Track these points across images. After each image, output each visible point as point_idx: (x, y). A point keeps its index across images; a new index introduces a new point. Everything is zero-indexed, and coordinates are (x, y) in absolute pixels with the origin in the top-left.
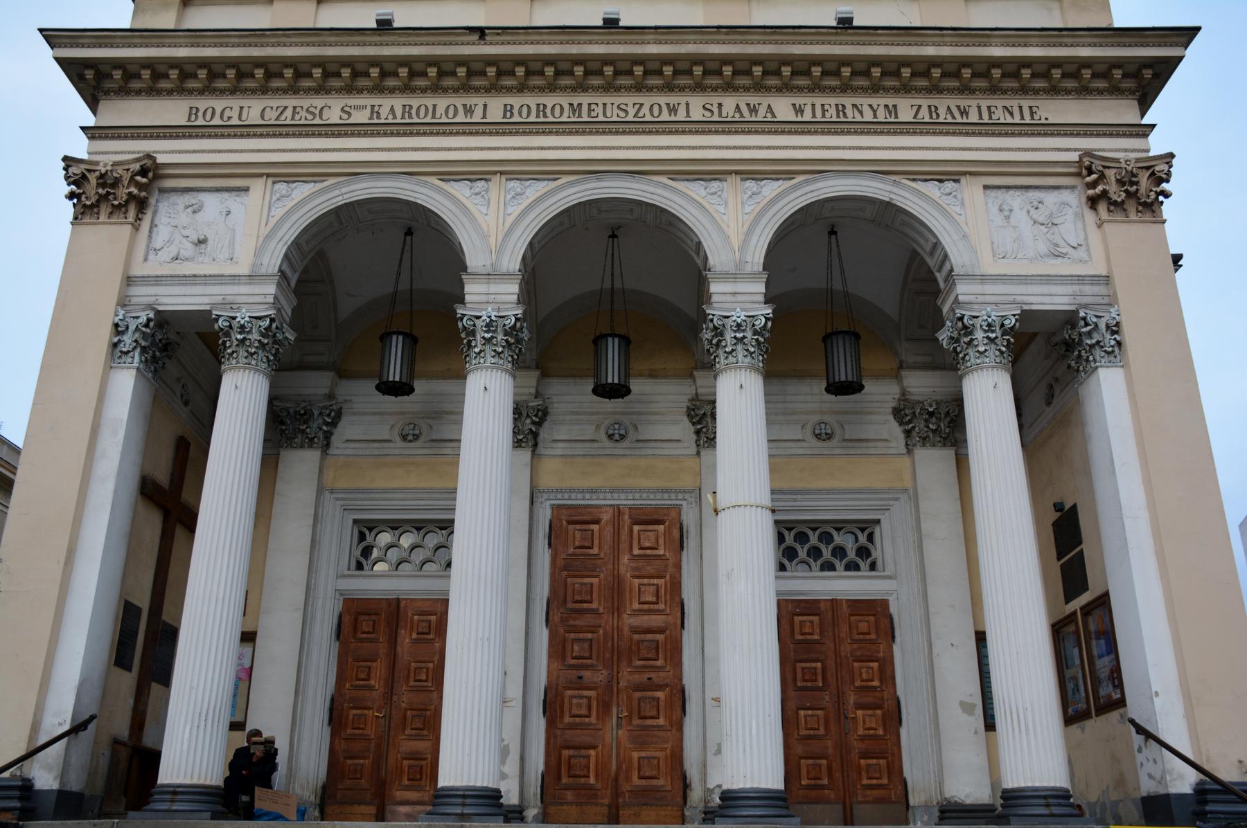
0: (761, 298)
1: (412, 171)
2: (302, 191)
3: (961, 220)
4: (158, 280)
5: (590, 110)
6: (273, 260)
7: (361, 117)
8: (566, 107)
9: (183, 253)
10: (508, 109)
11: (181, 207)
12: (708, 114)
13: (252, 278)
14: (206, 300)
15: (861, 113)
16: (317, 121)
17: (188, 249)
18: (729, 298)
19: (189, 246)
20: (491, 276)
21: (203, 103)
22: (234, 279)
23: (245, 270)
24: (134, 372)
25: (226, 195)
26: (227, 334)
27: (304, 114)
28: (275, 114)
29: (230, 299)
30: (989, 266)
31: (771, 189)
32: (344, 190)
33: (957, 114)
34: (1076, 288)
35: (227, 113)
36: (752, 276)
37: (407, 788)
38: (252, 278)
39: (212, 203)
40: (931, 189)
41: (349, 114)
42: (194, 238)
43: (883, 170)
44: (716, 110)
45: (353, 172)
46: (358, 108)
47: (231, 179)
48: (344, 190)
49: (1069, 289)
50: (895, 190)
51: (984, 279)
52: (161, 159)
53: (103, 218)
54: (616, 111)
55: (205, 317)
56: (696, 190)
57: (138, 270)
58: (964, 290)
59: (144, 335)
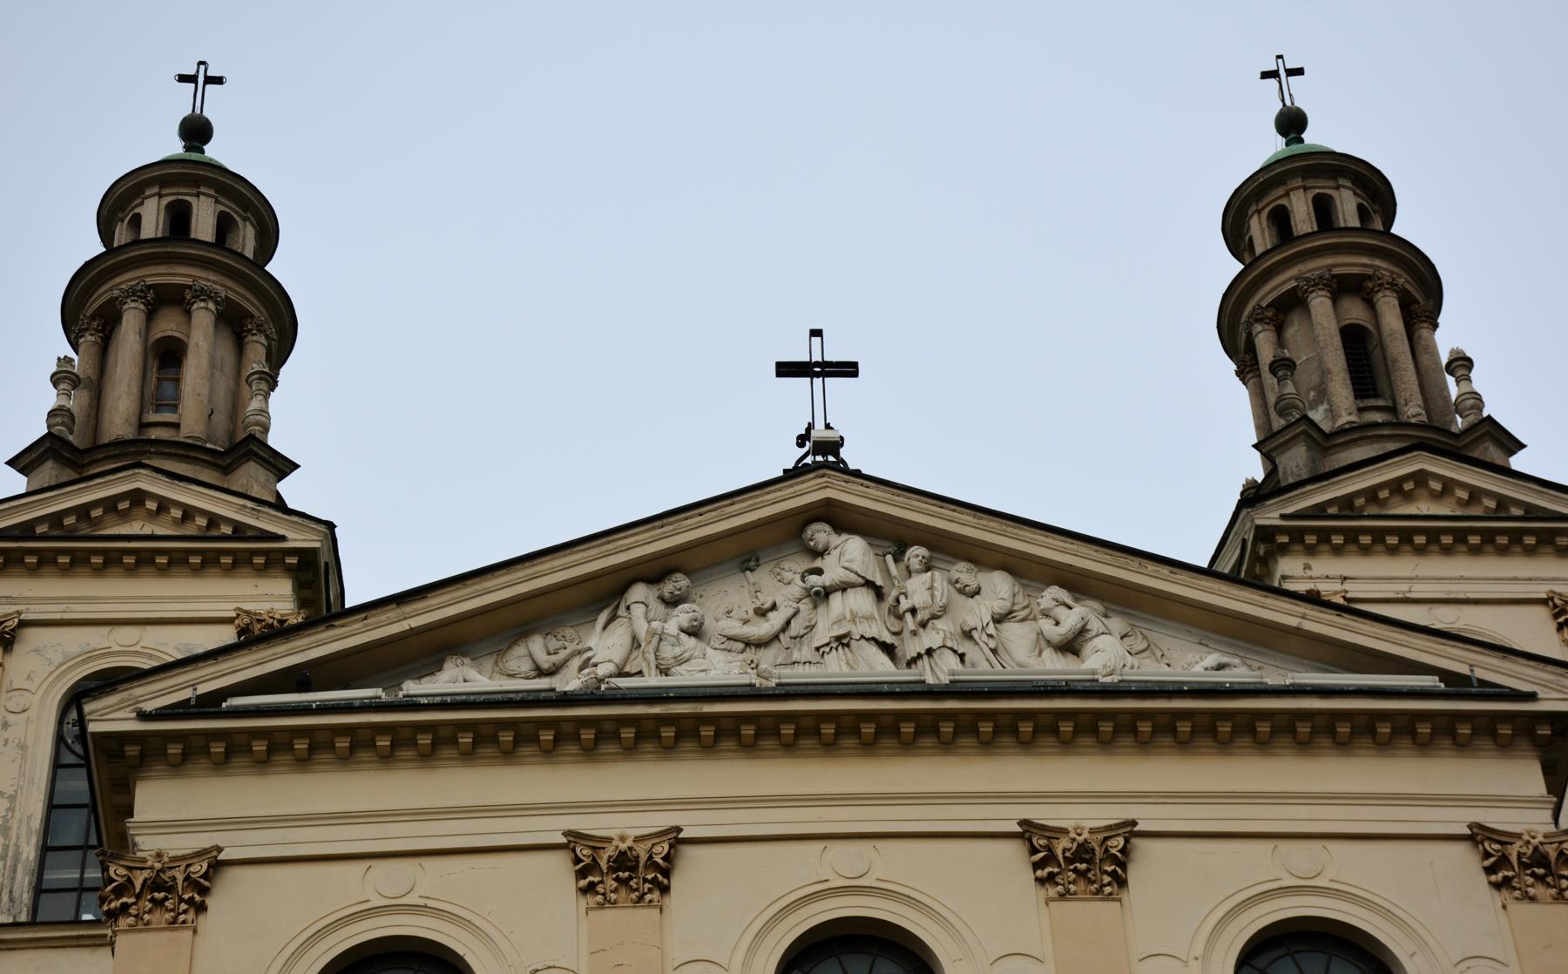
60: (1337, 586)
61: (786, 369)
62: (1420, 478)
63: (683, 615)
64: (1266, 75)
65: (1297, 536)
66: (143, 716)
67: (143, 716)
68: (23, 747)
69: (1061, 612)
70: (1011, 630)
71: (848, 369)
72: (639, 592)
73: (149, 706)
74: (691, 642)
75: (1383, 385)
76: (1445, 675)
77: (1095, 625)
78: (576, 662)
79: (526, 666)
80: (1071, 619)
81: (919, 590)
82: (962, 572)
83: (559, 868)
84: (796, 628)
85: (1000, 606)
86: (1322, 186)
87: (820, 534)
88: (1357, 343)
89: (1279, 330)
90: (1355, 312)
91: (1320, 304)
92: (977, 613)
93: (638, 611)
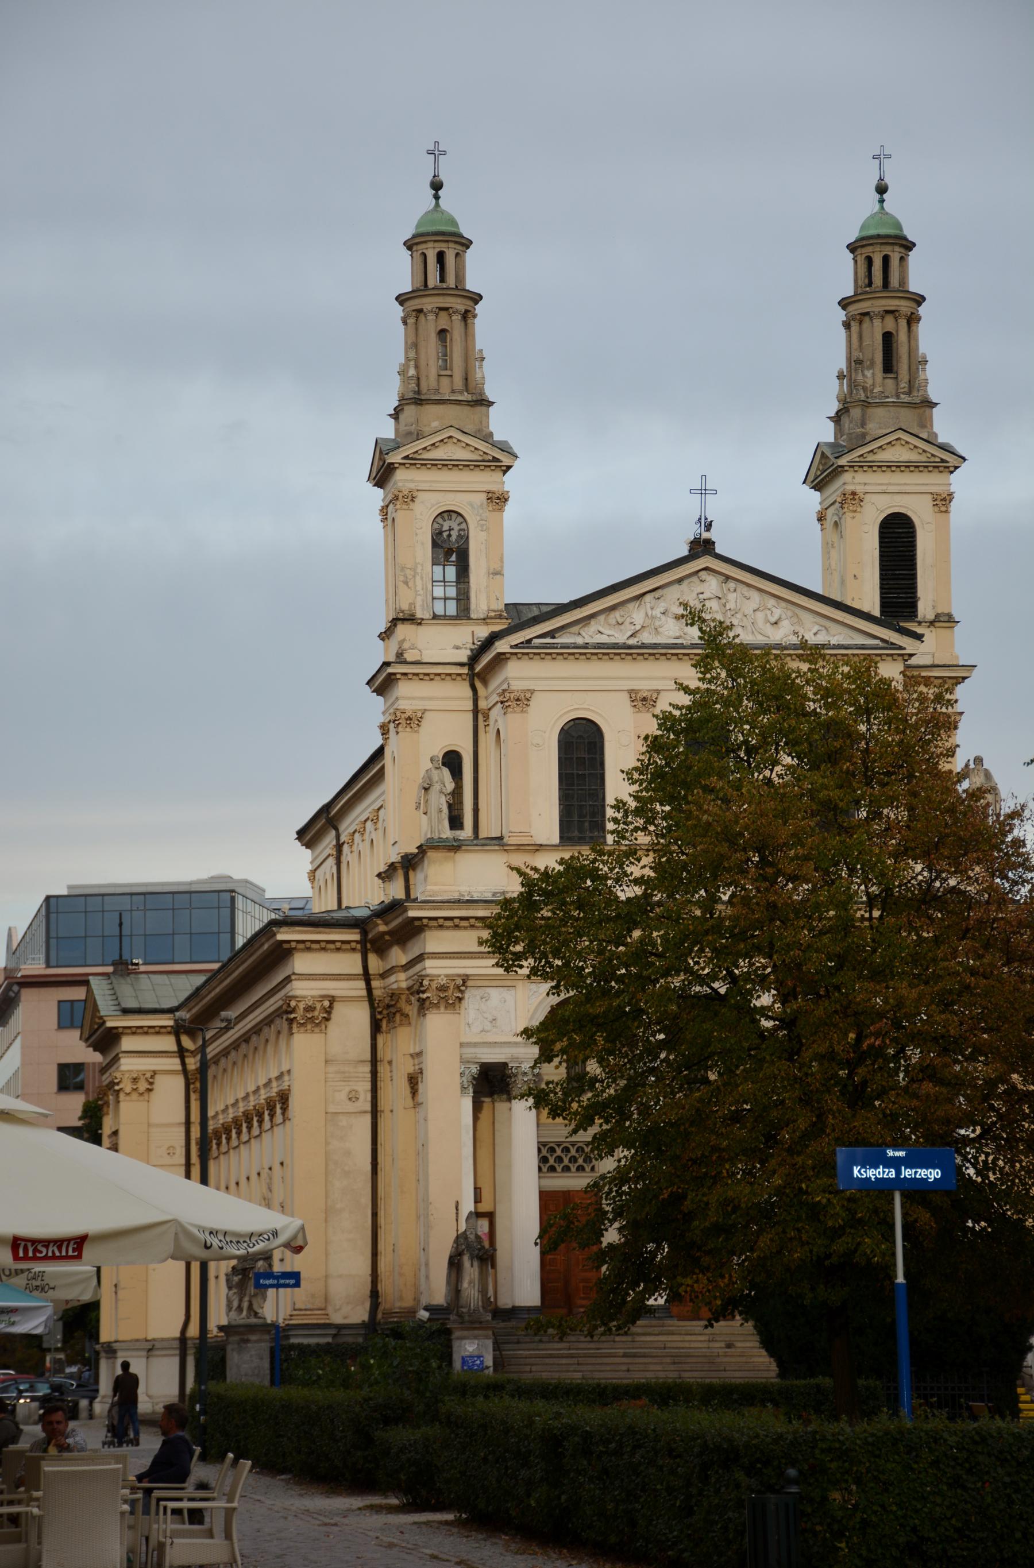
4: (475, 1045)
9: (486, 1028)
11: (478, 998)
14: (503, 1056)
17: (488, 1026)
19: (489, 1024)
24: (471, 1099)
25: (502, 989)
26: (516, 1075)
29: (516, 1055)
37: (584, 1299)
42: (490, 1018)
52: (469, 972)
53: (442, 1009)
57: (464, 1040)
59: (474, 1078)
60: (862, 487)
63: (662, 606)
66: (512, 647)
67: (512, 647)
68: (423, 544)
69: (774, 609)
70: (758, 613)
72: (648, 598)
73: (513, 643)
74: (663, 617)
75: (895, 369)
76: (883, 640)
77: (784, 616)
79: (614, 622)
80: (777, 613)
81: (732, 597)
82: (745, 590)
83: (626, 696)
85: (756, 606)
86: (887, 250)
87: (703, 575)
88: (888, 338)
89: (861, 322)
90: (890, 324)
91: (877, 322)
92: (749, 607)
93: (648, 605)
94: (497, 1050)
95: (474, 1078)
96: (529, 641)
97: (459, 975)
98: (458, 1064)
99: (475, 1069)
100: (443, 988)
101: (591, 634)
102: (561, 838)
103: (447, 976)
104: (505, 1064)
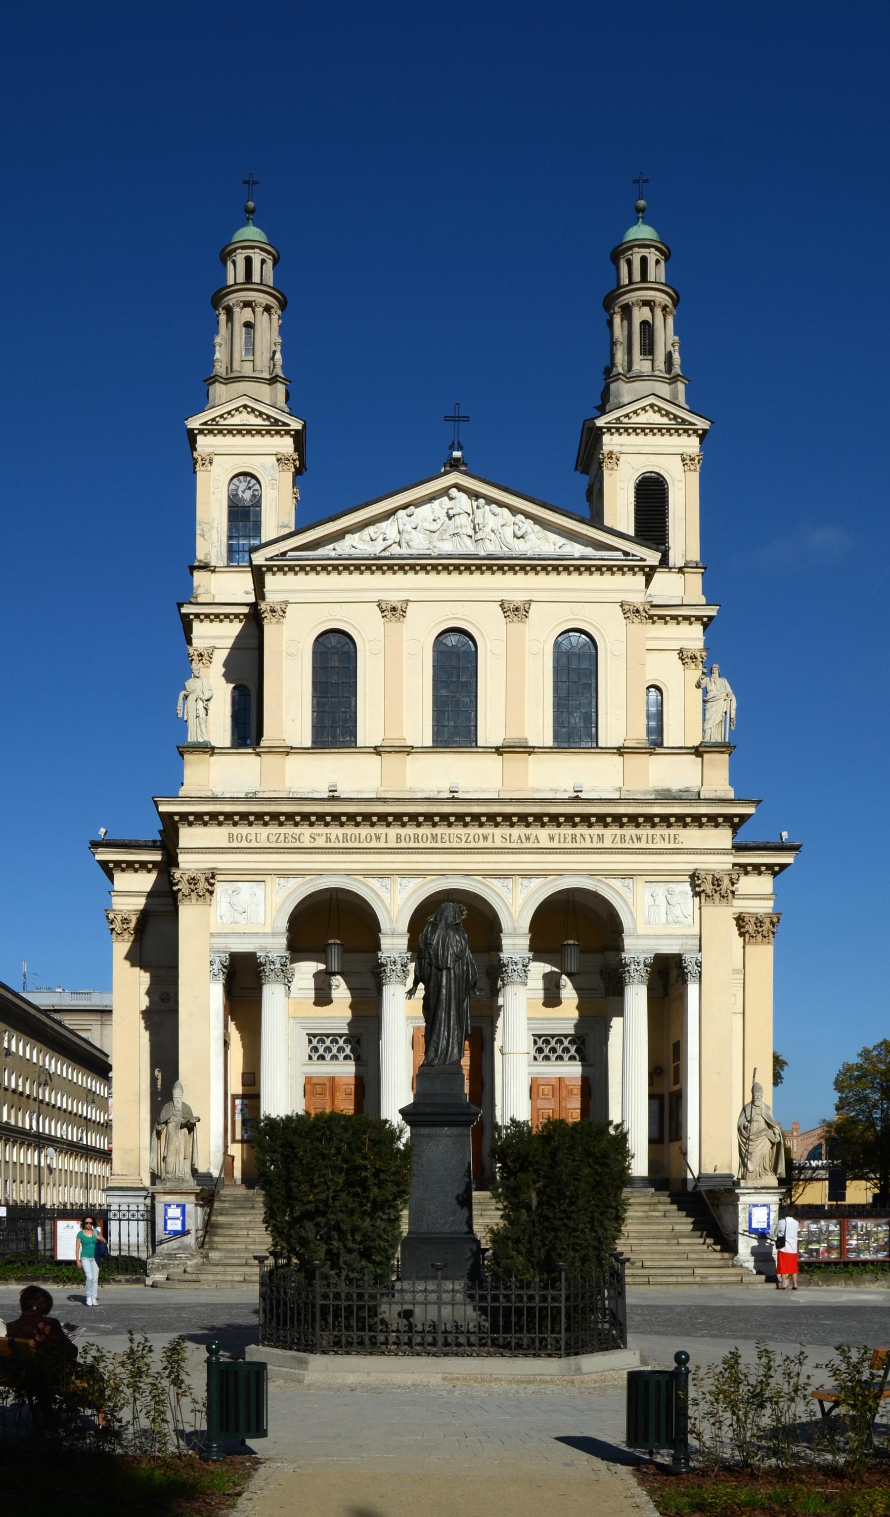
0: (527, 947)
1: (349, 874)
2: (293, 883)
3: (630, 901)
4: (226, 935)
5: (442, 838)
6: (283, 924)
7: (321, 842)
8: (429, 836)
10: (398, 838)
12: (504, 840)
13: (274, 935)
14: (252, 946)
15: (584, 839)
16: (298, 845)
18: (511, 947)
20: (393, 934)
21: (236, 830)
22: (265, 935)
23: (268, 930)
26: (265, 965)
27: (290, 838)
28: (275, 839)
30: (640, 931)
31: (535, 882)
32: (315, 883)
33: (635, 840)
34: (684, 941)
35: (249, 838)
36: (524, 935)
38: (274, 935)
39: (245, 888)
40: (616, 883)
41: (315, 839)
42: (241, 911)
43: (592, 874)
44: (508, 838)
45: (319, 873)
46: (319, 835)
47: (256, 876)
48: (315, 883)
49: (680, 942)
50: (599, 884)
51: (638, 937)
53: (194, 901)
54: (456, 839)
55: (252, 956)
56: (495, 883)
58: (628, 943)
61: (447, 419)
62: (652, 406)
64: (634, 182)
65: (609, 429)
71: (466, 419)
78: (381, 537)
84: (445, 527)
94: (247, 940)
95: (225, 967)
96: (284, 554)
97: (209, 869)
98: (208, 953)
99: (225, 957)
100: (193, 881)
101: (344, 547)
102: (313, 742)
103: (198, 870)
104: (254, 954)
